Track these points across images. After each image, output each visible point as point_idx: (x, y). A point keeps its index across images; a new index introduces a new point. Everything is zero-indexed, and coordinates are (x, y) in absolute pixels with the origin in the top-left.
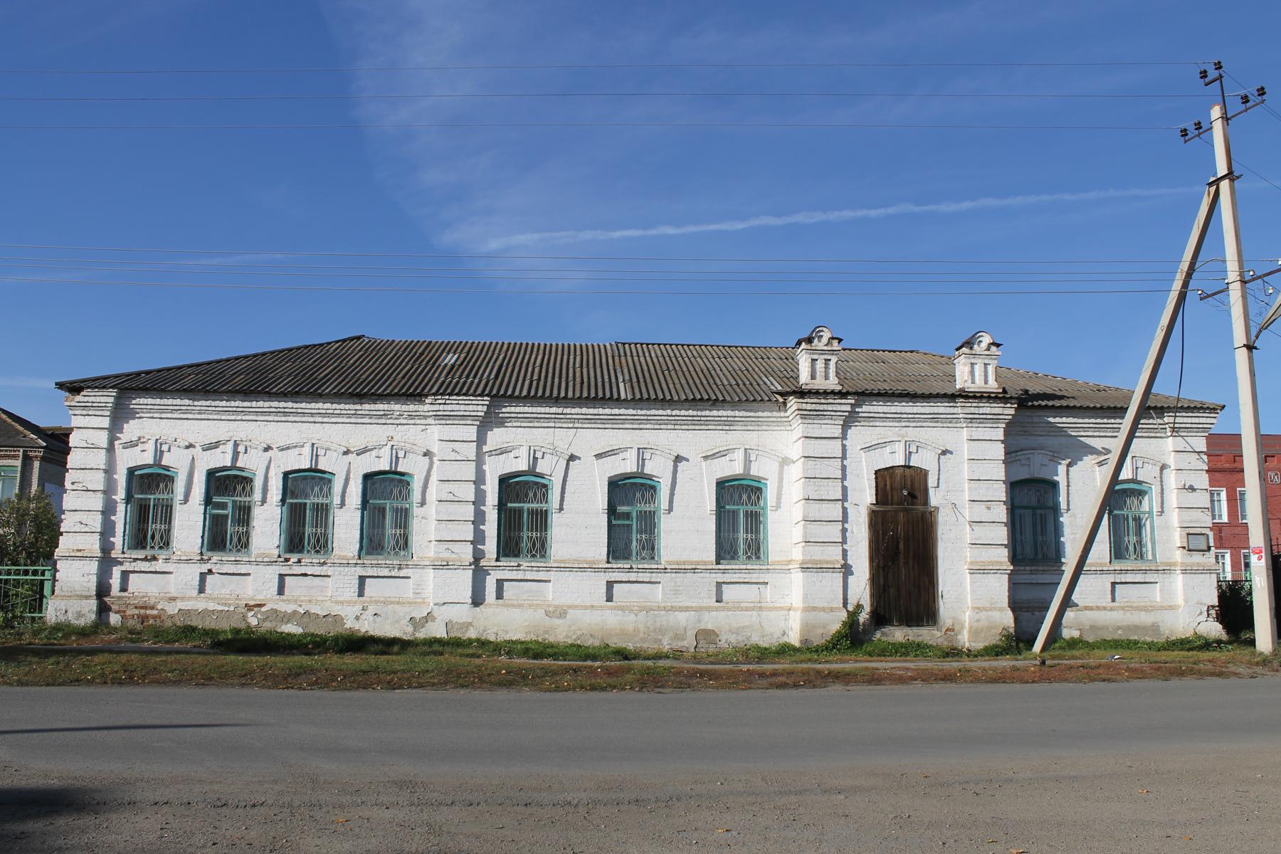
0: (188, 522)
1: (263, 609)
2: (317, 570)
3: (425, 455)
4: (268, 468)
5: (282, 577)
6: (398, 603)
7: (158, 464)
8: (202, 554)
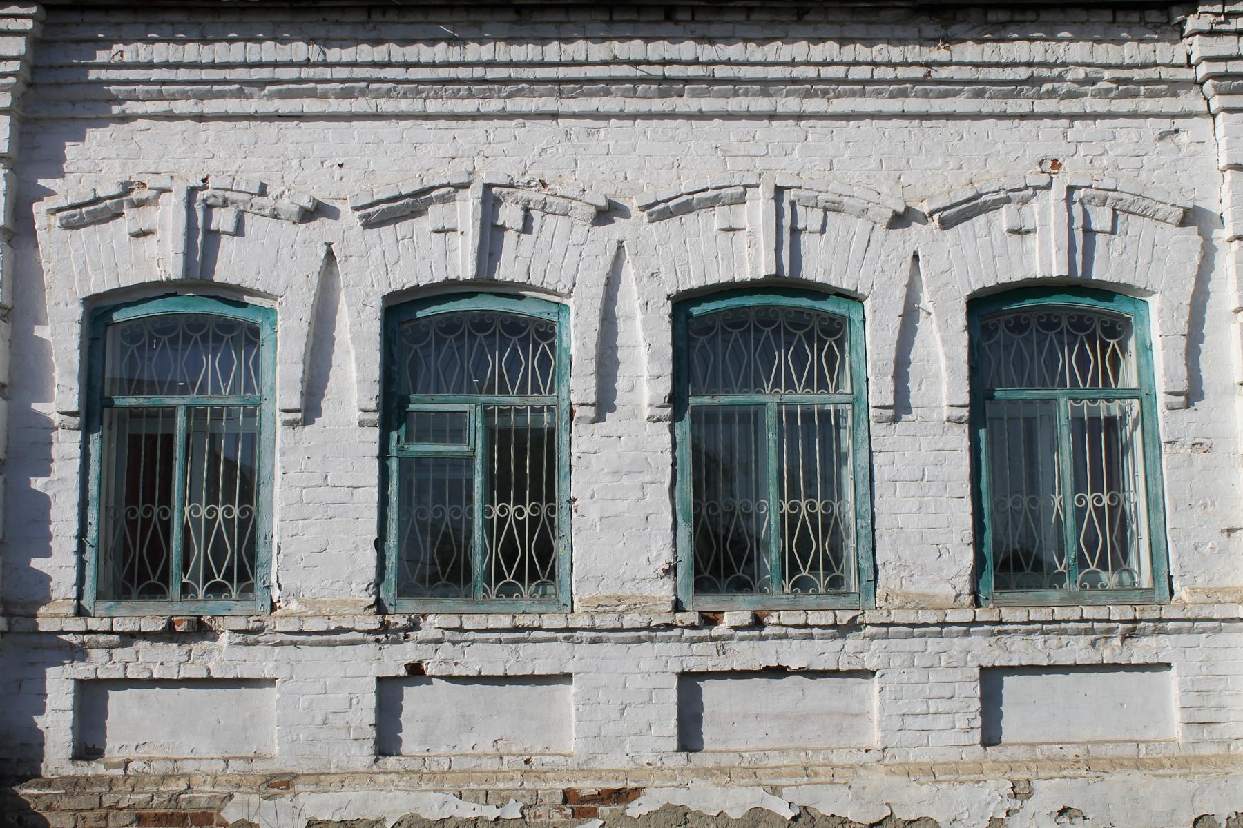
0: (322, 496)
1: (635, 809)
2: (822, 652)
3: (1183, 223)
4: (612, 284)
5: (689, 682)
6: (1139, 764)
7: (198, 278)
8: (380, 607)
